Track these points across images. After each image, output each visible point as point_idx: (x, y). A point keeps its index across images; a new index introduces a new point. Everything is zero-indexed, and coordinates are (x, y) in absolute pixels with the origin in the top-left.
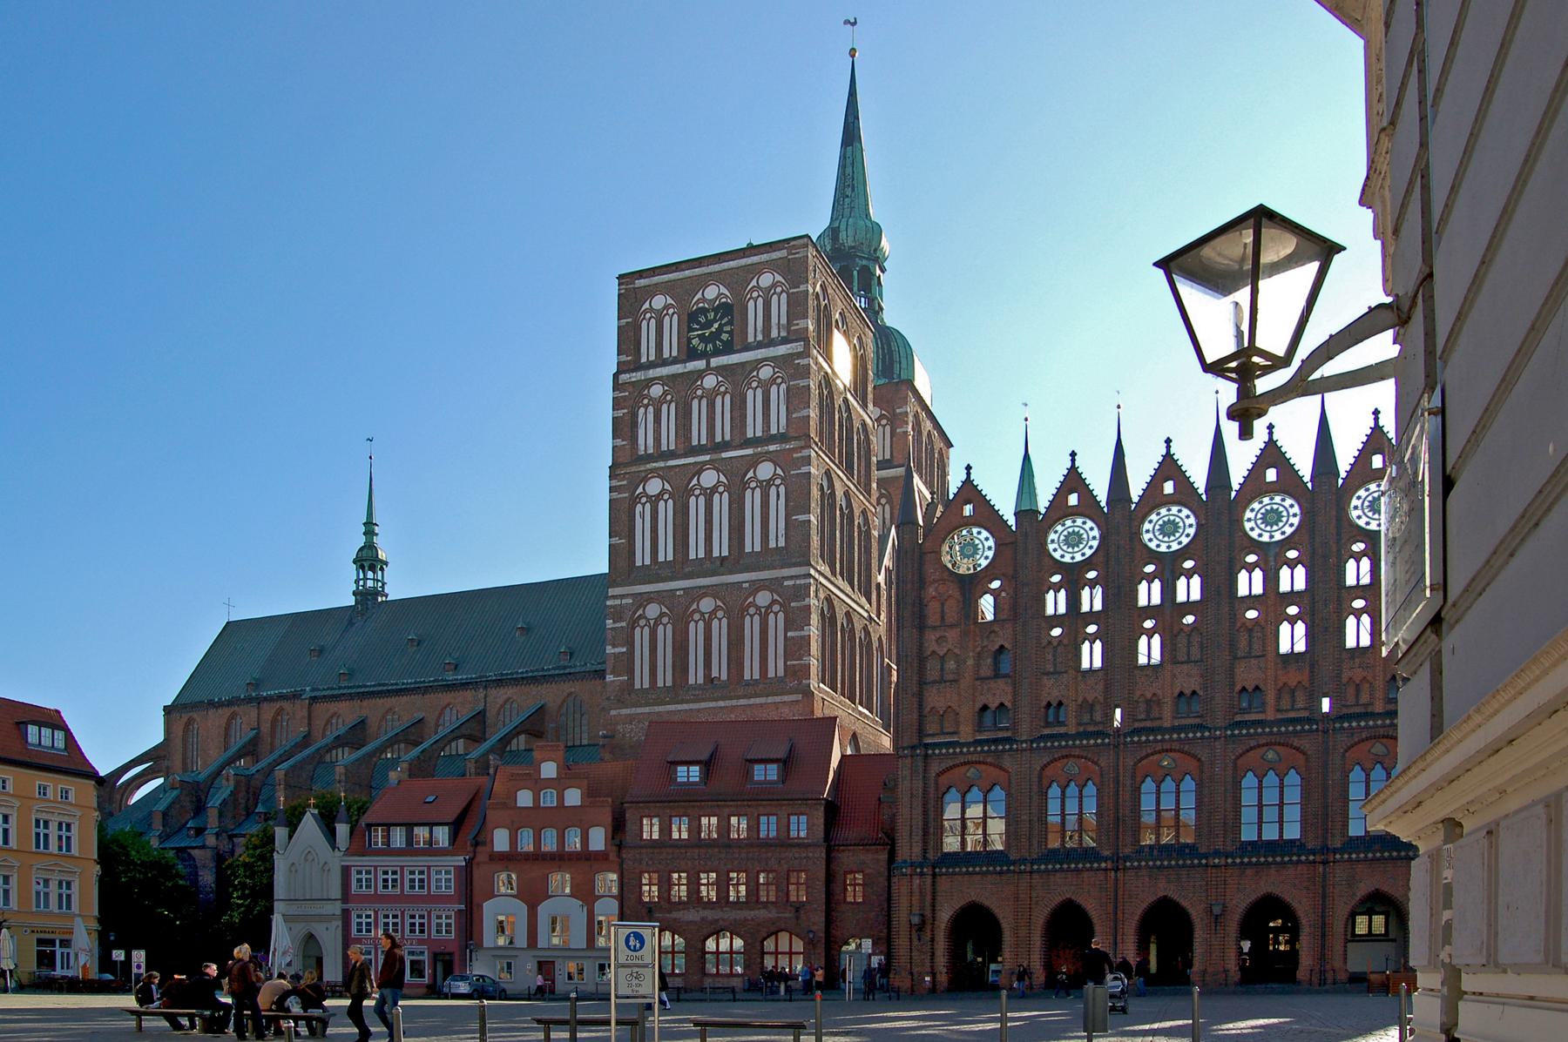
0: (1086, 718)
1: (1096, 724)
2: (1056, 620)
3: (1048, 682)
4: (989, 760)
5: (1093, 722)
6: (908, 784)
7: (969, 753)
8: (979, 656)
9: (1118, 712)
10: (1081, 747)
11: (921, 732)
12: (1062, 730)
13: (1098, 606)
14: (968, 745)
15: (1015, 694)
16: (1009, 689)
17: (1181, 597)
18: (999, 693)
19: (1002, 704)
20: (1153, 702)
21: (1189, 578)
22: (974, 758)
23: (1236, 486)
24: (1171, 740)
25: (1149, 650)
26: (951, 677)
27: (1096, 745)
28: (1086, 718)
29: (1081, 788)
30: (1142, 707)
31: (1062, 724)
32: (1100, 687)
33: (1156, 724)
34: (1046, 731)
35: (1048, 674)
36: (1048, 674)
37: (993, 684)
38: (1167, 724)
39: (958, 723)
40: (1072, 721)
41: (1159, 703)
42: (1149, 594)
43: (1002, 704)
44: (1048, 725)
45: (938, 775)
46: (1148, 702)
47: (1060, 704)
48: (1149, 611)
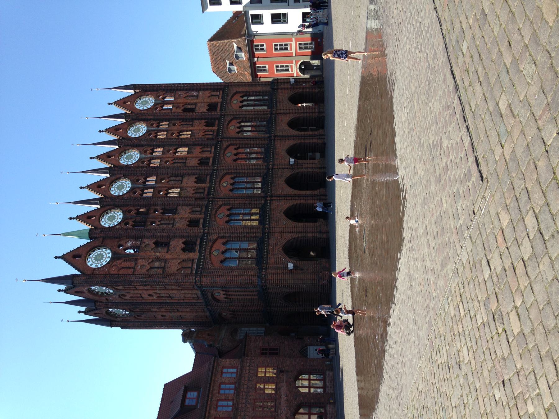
3: (178, 225)
4: (210, 244)
7: (205, 251)
10: (211, 211)
12: (202, 220)
16: (177, 240)
18: (178, 244)
19: (183, 243)
22: (208, 250)
24: (215, 182)
26: (163, 264)
27: (212, 206)
32: (185, 207)
33: (207, 189)
34: (201, 226)
43: (183, 243)
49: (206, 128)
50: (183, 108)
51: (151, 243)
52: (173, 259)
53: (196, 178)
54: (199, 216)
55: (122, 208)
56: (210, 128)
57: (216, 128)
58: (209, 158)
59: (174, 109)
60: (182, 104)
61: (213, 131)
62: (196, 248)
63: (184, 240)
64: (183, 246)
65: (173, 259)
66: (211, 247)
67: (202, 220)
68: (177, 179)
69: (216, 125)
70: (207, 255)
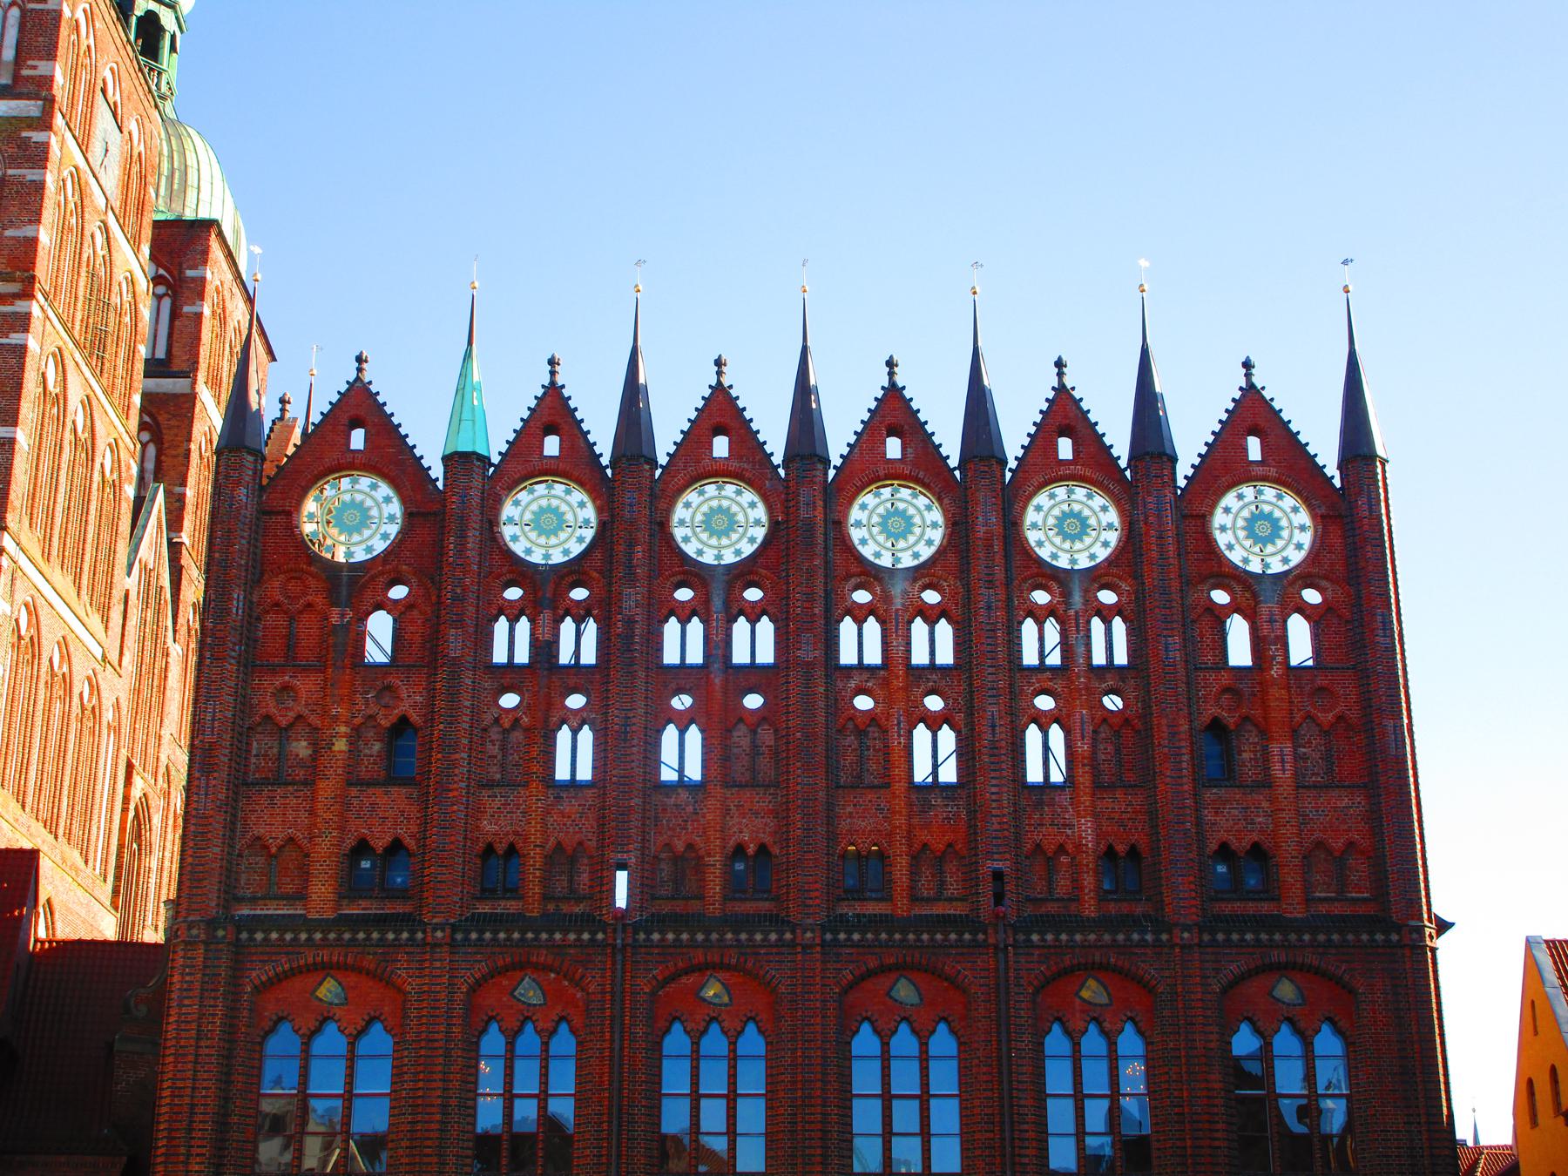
0: (560, 886)
1: (579, 900)
2: (510, 676)
3: (493, 802)
4: (369, 961)
5: (573, 896)
6: (188, 1011)
8: (355, 736)
9: (622, 878)
11: (231, 896)
12: (509, 906)
13: (589, 657)
14: (325, 926)
15: (424, 823)
17: (740, 655)
20: (689, 862)
21: (753, 621)
23: (836, 461)
25: (682, 754)
28: (560, 886)
29: (547, 1035)
30: (665, 870)
31: (513, 892)
33: (695, 906)
34: (484, 908)
35: (491, 784)
36: (491, 784)
37: (377, 795)
38: (714, 909)
39: (305, 876)
40: (534, 889)
41: (700, 868)
42: (682, 643)
44: (487, 893)
45: (262, 989)
46: (676, 859)
47: (512, 850)
48: (683, 676)
49: (1088, 860)
50: (1230, 720)
51: (404, 707)
52: (312, 813)
53: (763, 849)
54: (534, 889)
55: (598, 555)
56: (1088, 880)
57: (1090, 909)
58: (888, 898)
59: (1225, 679)
60: (1256, 712)
61: (1075, 897)
62: (363, 903)
63: (410, 842)
64: (380, 844)
65: (312, 813)
66: (358, 969)
67: (509, 906)
68: (764, 762)
69: (1113, 908)
70: (309, 957)
